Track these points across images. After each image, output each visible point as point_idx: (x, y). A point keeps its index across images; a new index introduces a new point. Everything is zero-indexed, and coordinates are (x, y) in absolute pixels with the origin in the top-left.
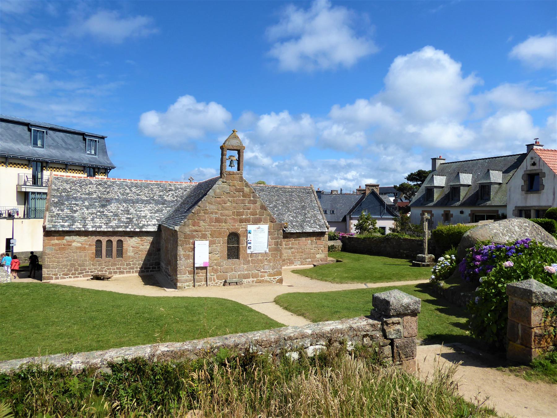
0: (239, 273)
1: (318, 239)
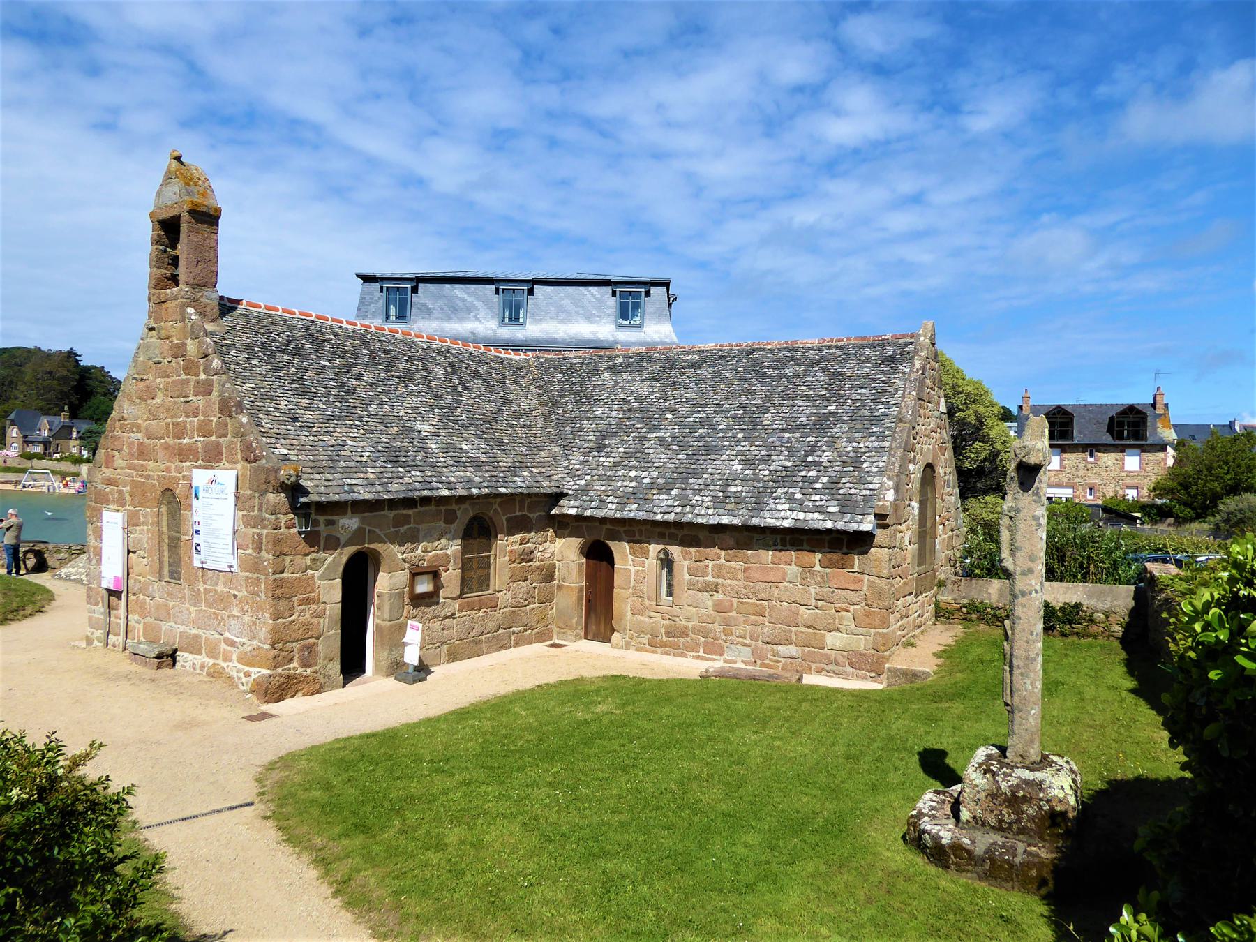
0: (182, 628)
1: (833, 564)
